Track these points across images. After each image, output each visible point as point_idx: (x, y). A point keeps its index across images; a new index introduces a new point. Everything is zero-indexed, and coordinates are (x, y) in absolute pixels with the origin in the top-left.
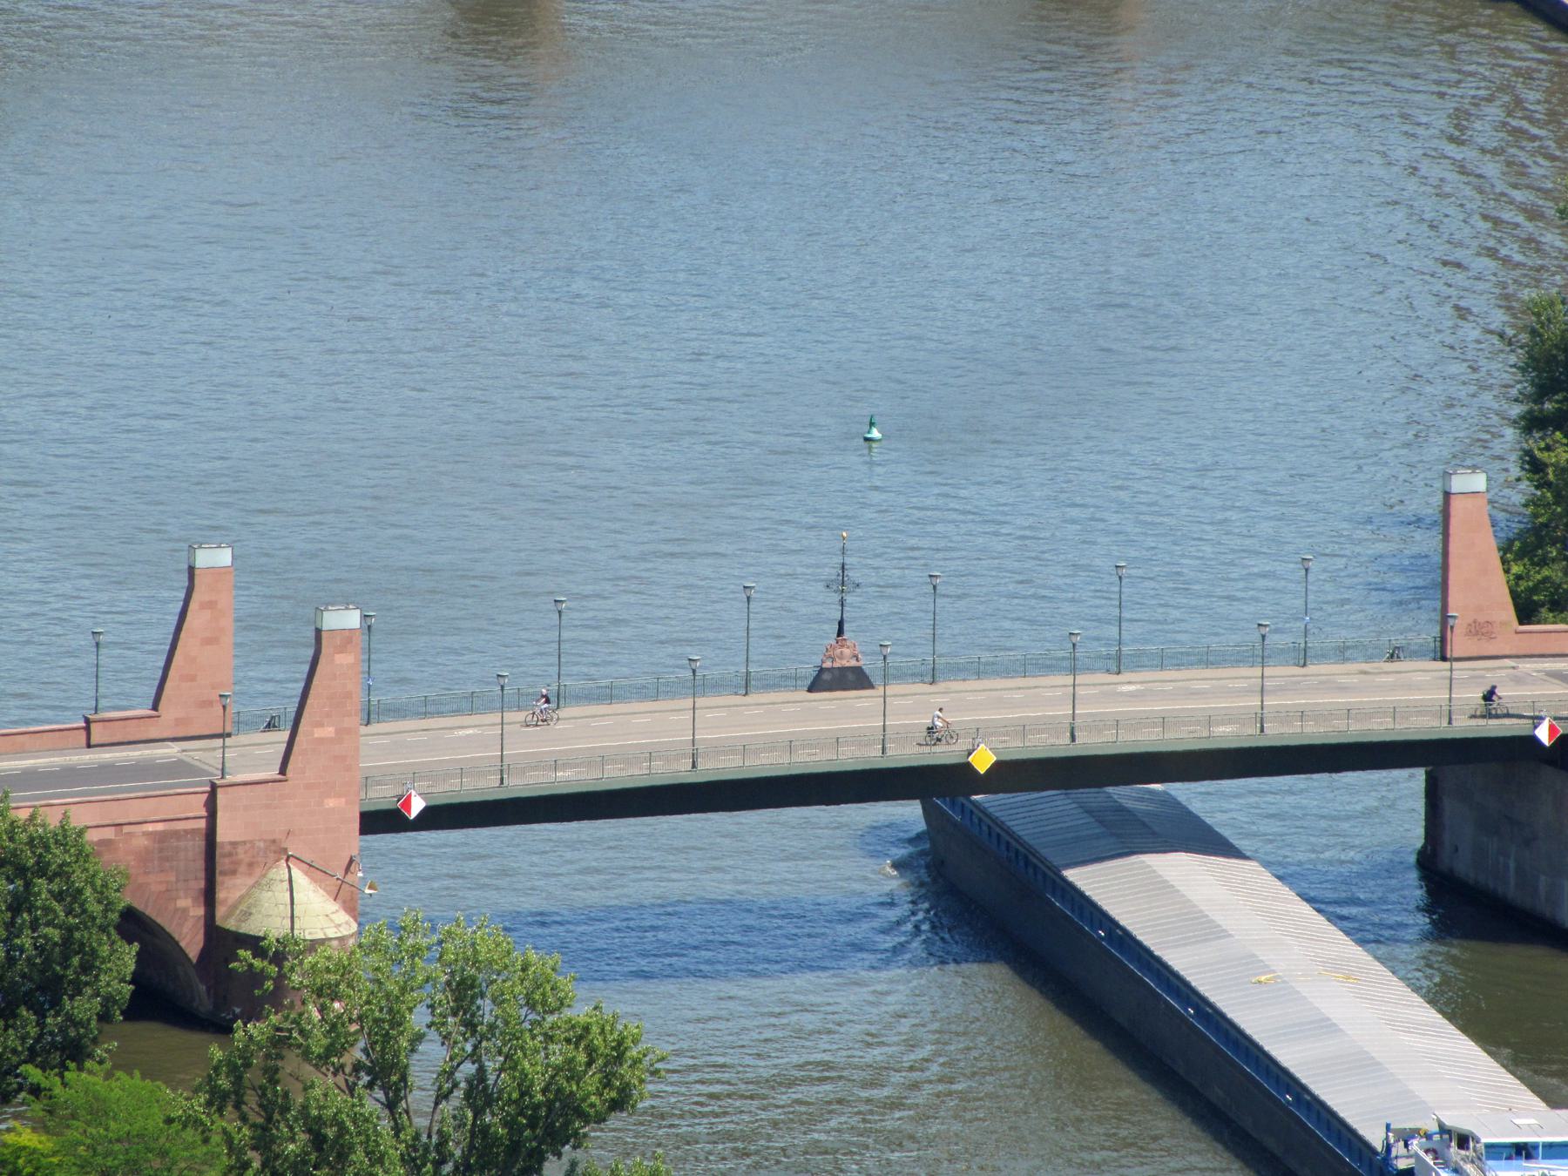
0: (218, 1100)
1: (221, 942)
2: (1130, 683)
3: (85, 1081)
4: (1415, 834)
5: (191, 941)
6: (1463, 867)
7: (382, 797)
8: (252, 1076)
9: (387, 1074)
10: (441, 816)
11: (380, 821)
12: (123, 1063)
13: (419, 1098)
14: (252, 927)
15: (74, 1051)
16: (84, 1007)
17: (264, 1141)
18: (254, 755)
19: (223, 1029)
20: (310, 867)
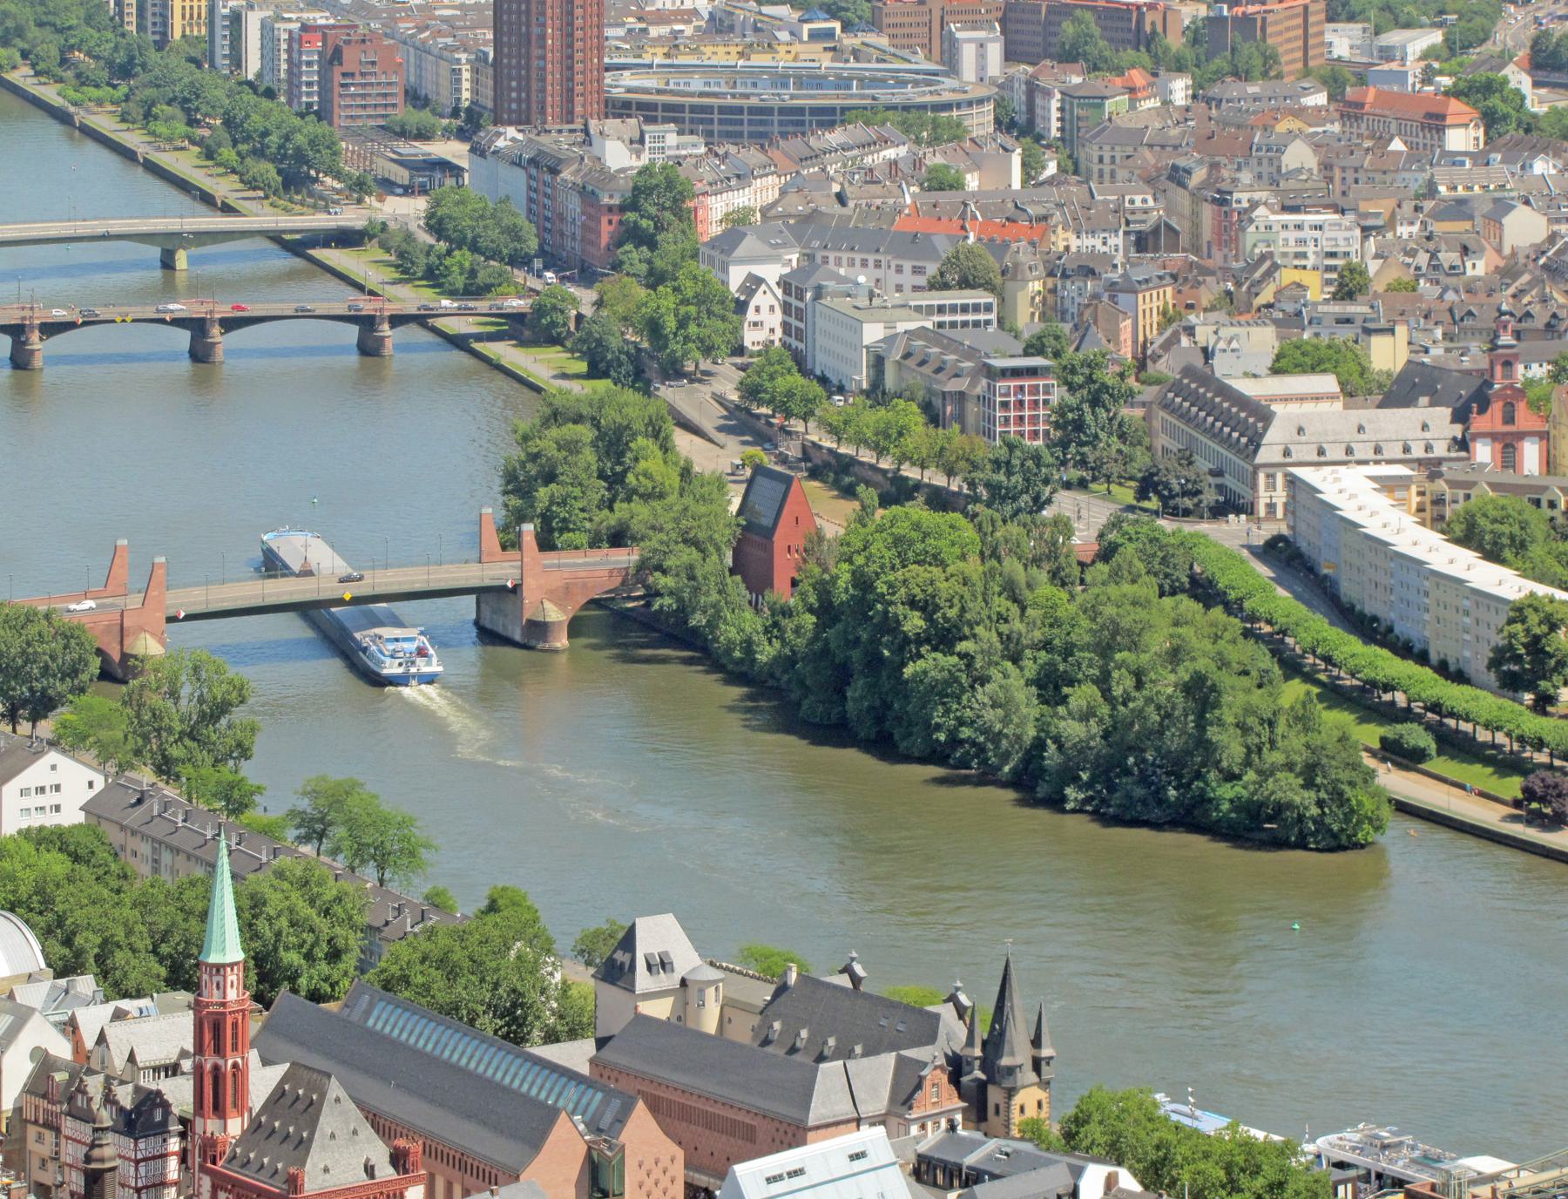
0: (125, 703)
1: (125, 657)
2: (390, 572)
3: (85, 699)
4: (474, 616)
5: (116, 656)
6: (488, 625)
7: (172, 613)
8: (135, 697)
9: (174, 694)
10: (189, 618)
11: (172, 619)
12: (97, 693)
13: (183, 702)
14: (134, 652)
15: (82, 690)
16: (84, 677)
17: (138, 716)
18: (134, 601)
19: (126, 682)
20: (153, 634)
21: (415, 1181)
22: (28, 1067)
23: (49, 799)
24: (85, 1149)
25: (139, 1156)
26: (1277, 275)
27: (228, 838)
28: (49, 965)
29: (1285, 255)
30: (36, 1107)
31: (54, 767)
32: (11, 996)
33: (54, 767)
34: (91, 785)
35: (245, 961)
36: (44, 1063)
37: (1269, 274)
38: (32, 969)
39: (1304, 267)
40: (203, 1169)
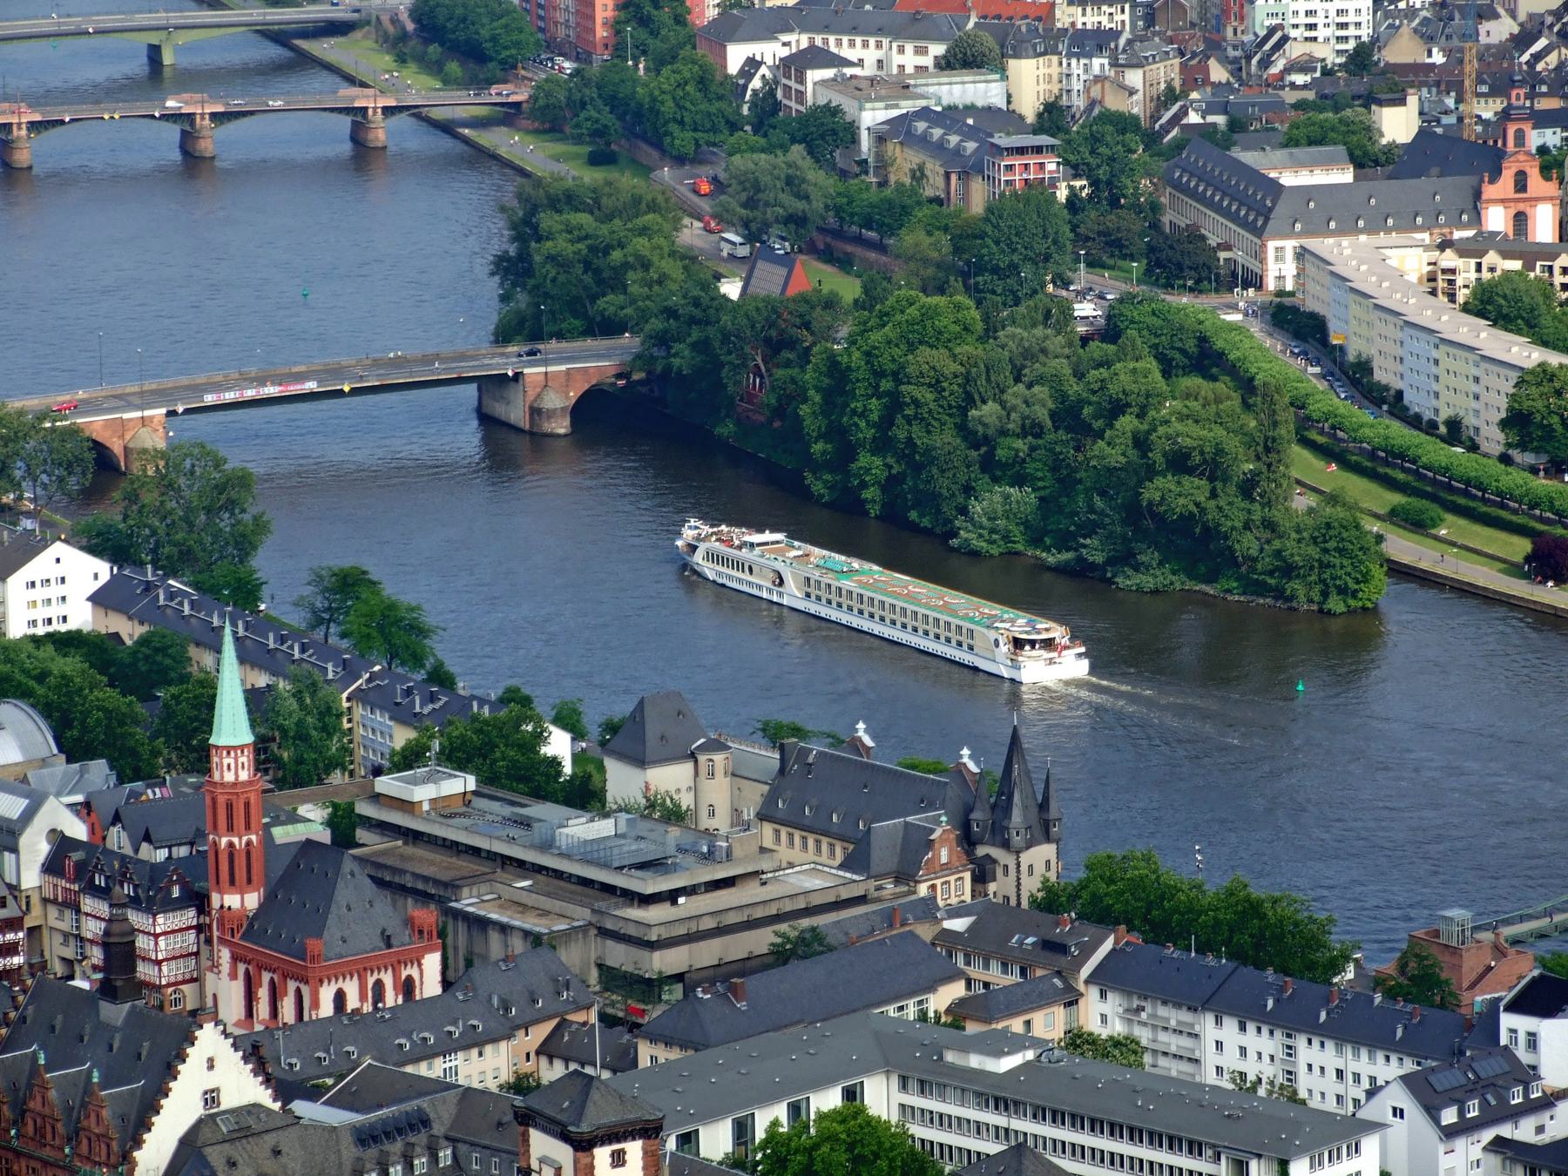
21: (431, 950)
22: (44, 848)
23: (55, 591)
24: (103, 925)
25: (158, 930)
26: (1287, 47)
27: (234, 624)
28: (61, 750)
29: (1296, 26)
30: (55, 886)
31: (58, 560)
32: (25, 780)
33: (58, 560)
34: (96, 576)
35: (255, 743)
36: (62, 844)
37: (1279, 45)
38: (45, 753)
39: (1315, 39)
40: (222, 941)
